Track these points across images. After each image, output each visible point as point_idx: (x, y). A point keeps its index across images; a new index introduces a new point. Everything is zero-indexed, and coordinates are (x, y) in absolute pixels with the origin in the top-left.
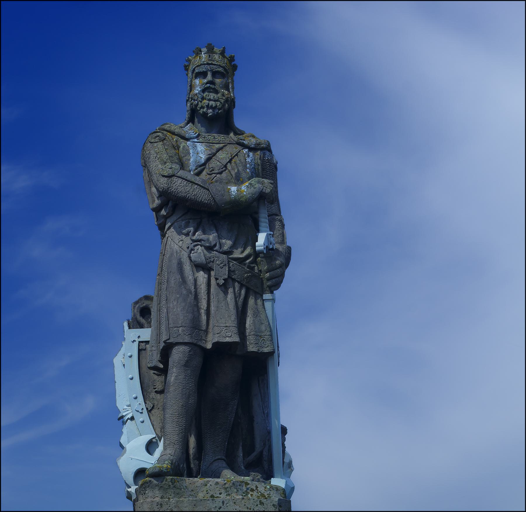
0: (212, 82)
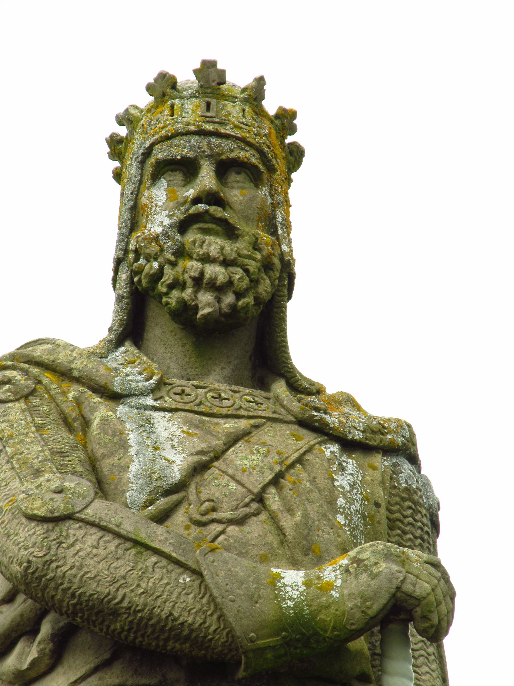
0: (213, 198)
